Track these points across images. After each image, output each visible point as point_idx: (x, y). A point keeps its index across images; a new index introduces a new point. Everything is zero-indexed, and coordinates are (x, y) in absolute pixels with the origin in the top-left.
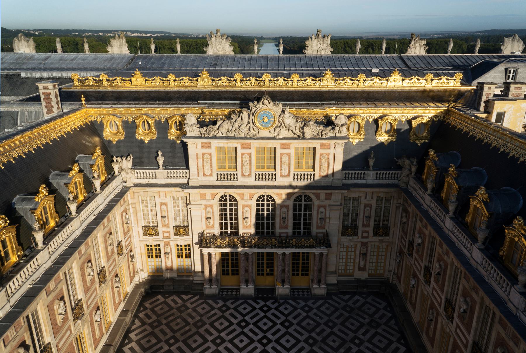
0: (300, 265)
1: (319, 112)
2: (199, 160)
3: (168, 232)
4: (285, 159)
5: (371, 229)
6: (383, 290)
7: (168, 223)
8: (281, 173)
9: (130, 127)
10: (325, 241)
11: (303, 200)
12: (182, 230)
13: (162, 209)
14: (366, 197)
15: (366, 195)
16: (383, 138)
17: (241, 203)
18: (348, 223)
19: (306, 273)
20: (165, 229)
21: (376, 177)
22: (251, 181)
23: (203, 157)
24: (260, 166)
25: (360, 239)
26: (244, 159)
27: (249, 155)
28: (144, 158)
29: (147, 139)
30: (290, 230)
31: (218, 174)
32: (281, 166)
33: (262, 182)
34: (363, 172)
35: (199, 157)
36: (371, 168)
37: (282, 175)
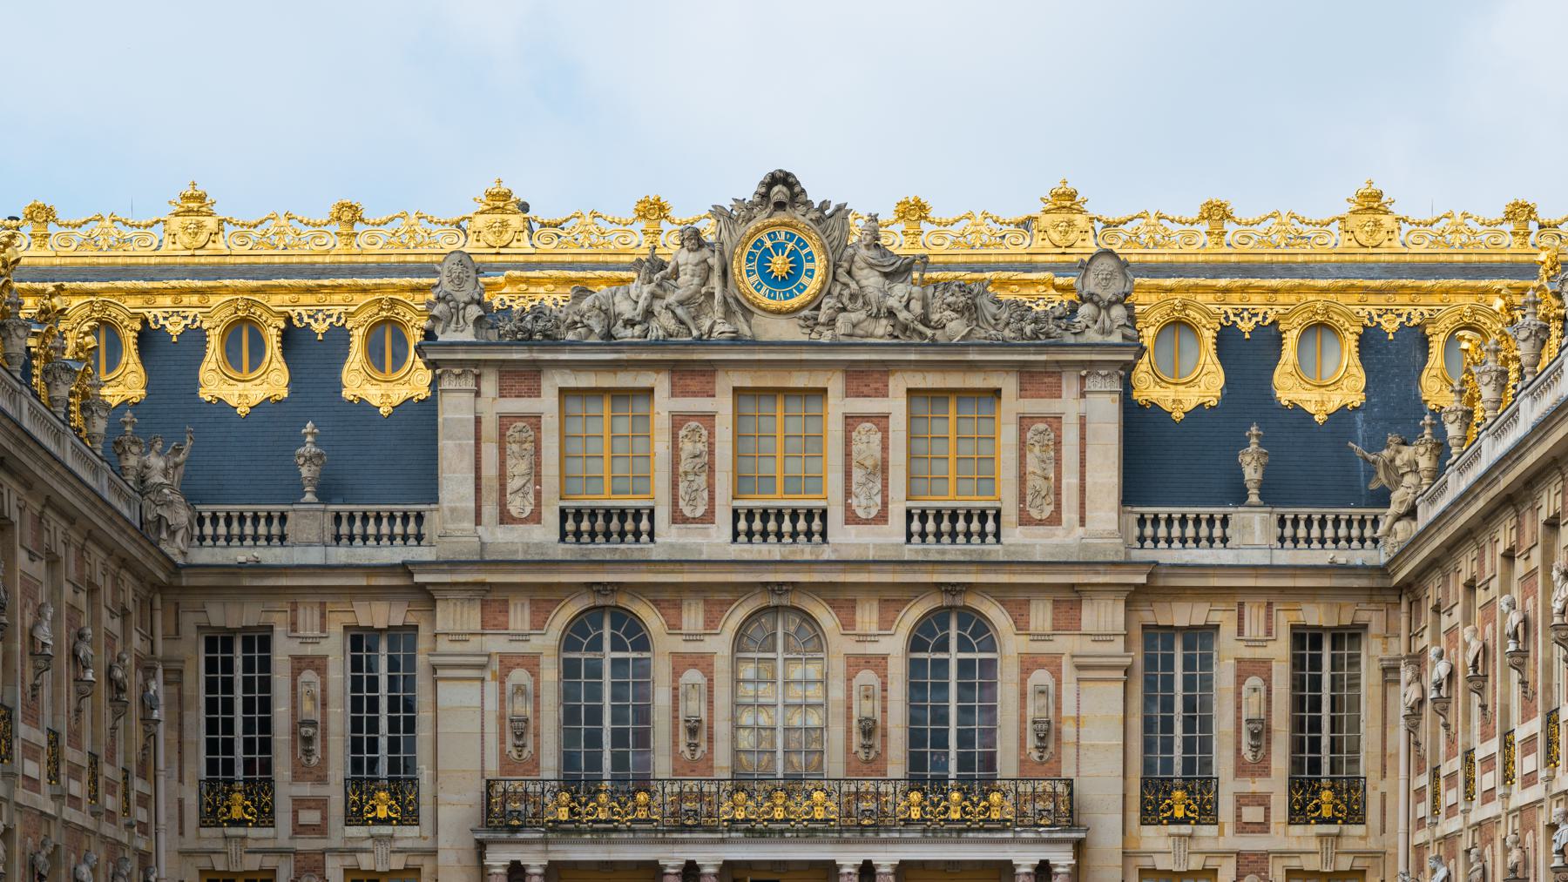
2: (484, 446)
4: (867, 443)
5: (1276, 784)
7: (324, 759)
8: (848, 507)
13: (302, 689)
14: (1240, 631)
15: (1241, 618)
20: (306, 790)
21: (1282, 539)
23: (502, 435)
25: (1232, 840)
26: (687, 447)
31: (563, 514)
32: (848, 475)
33: (764, 547)
34: (1218, 511)
35: (484, 434)
36: (1254, 498)
37: (851, 518)
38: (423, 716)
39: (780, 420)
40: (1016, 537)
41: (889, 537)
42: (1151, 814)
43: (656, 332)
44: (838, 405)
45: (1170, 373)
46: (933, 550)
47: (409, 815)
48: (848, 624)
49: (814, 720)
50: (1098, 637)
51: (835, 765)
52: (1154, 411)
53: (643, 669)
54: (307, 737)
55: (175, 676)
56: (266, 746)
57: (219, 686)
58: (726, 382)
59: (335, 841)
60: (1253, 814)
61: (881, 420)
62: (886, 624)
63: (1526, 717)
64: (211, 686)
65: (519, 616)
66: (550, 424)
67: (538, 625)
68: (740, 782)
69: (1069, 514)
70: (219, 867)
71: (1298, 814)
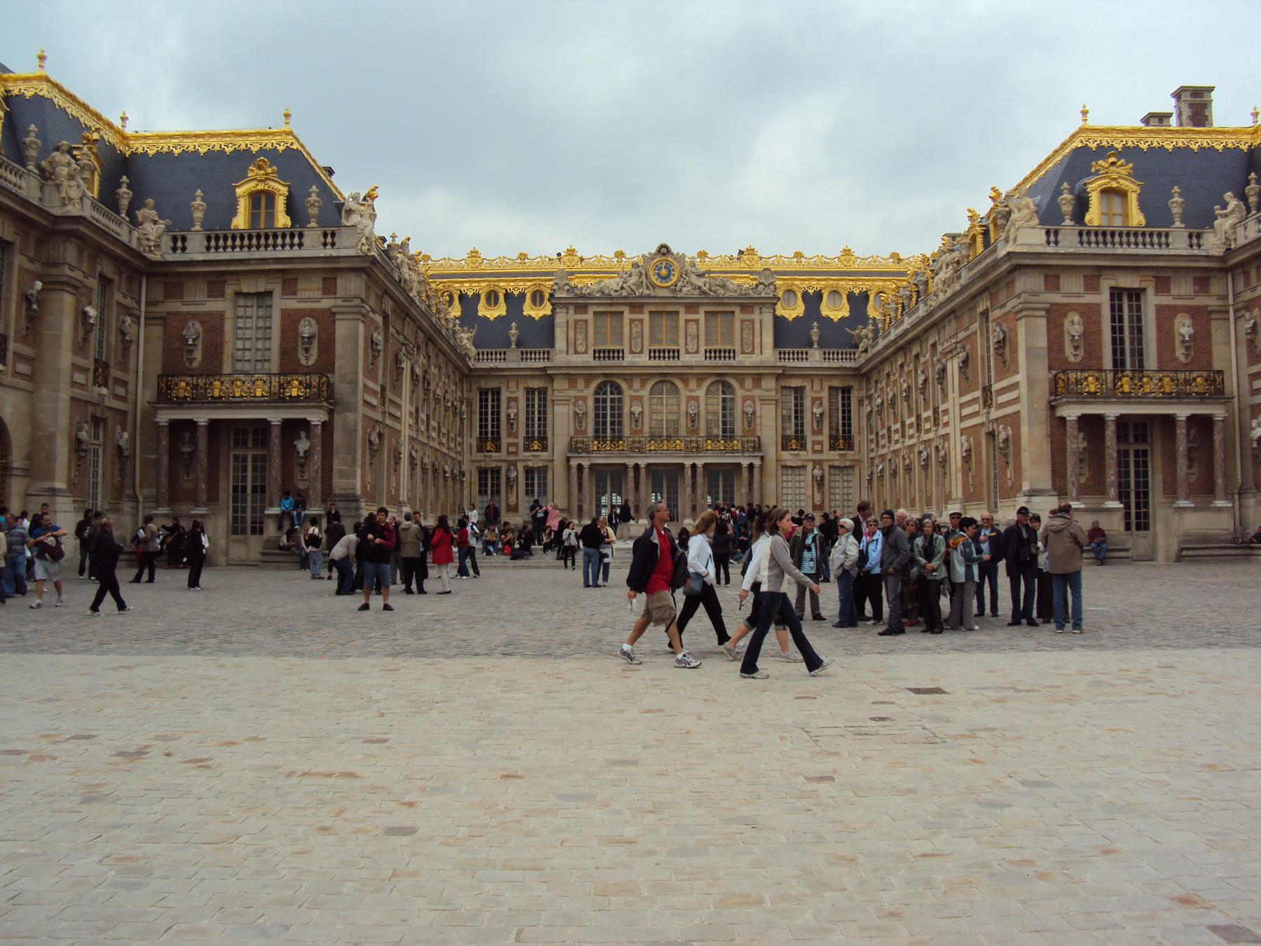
3: (516, 445)
4: (692, 328)
20: (511, 440)
26: (634, 330)
37: (687, 352)
38: (549, 416)
39: (665, 322)
40: (741, 359)
41: (699, 359)
42: (785, 448)
43: (625, 294)
44: (683, 316)
45: (788, 305)
46: (713, 362)
47: (544, 449)
48: (686, 386)
49: (675, 417)
50: (767, 390)
51: (683, 432)
53: (620, 400)
54: (510, 425)
55: (470, 404)
56: (498, 426)
57: (483, 406)
58: (647, 309)
59: (520, 457)
60: (817, 447)
61: (697, 321)
62: (699, 386)
63: (910, 416)
64: (481, 407)
65: (581, 384)
66: (591, 322)
67: (587, 386)
68: (652, 437)
69: (757, 351)
70: (483, 465)
71: (832, 448)
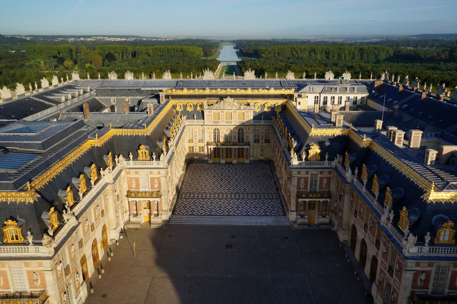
0: (241, 153)
1: (245, 101)
5: (264, 141)
6: (269, 163)
9: (185, 106)
10: (248, 144)
11: (240, 130)
12: (201, 141)
16: (266, 110)
17: (221, 131)
18: (256, 139)
19: (243, 157)
22: (224, 124)
24: (227, 119)
27: (223, 115)
28: (190, 116)
29: (190, 111)
30: (237, 141)
52: (256, 112)
